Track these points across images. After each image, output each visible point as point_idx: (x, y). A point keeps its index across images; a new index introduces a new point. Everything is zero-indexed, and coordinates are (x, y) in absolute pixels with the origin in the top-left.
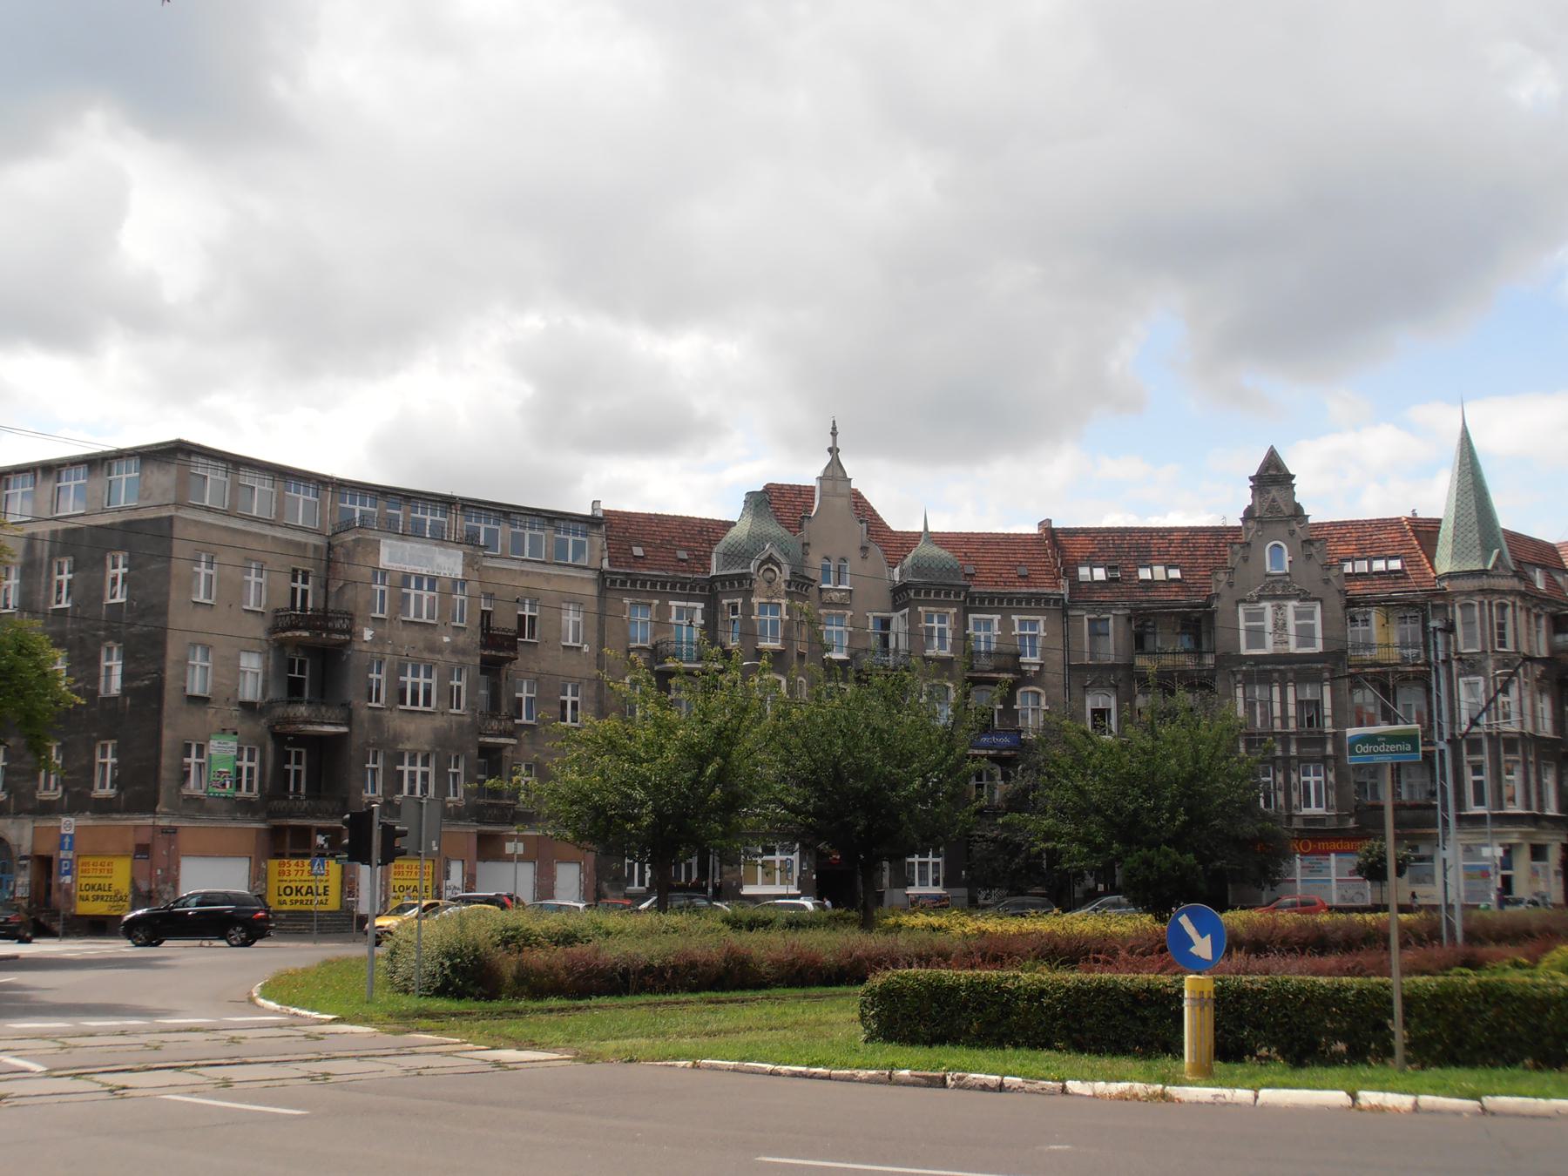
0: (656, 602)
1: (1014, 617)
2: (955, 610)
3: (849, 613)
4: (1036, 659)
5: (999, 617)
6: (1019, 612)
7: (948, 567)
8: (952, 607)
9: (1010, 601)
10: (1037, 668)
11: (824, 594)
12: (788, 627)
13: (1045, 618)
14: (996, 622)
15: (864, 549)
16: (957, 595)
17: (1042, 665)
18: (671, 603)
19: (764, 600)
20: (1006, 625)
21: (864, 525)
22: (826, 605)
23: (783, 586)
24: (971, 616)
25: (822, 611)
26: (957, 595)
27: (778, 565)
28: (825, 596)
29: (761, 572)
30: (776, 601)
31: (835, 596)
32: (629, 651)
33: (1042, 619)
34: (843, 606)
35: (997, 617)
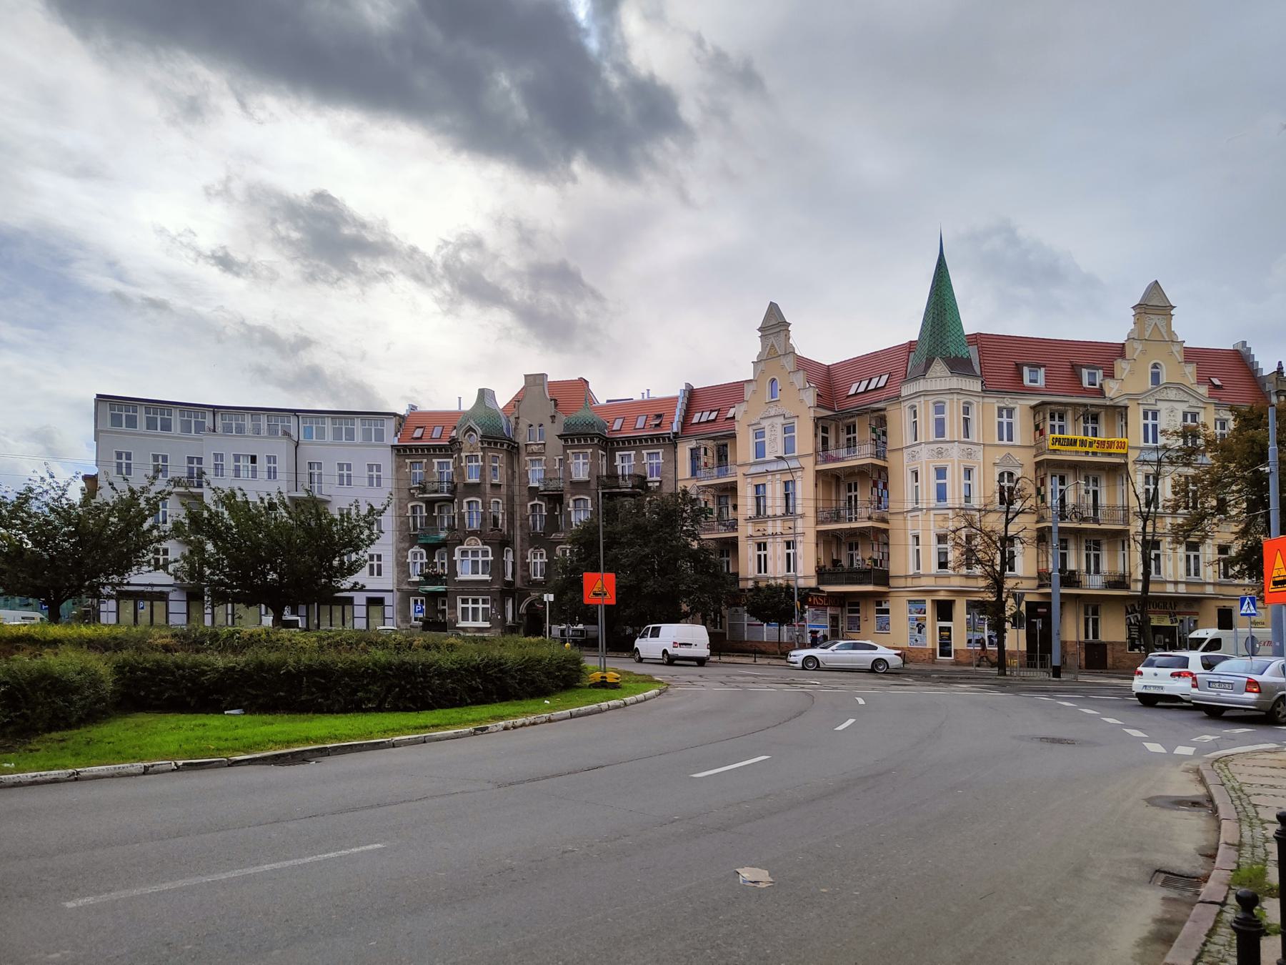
0: (425, 460)
1: (643, 452)
2: (591, 450)
3: (544, 458)
4: (659, 479)
5: (634, 452)
6: (647, 447)
7: (587, 422)
8: (589, 448)
9: (640, 441)
10: (658, 484)
11: (528, 448)
12: (483, 469)
13: (663, 450)
14: (632, 456)
15: (553, 417)
16: (592, 440)
17: (660, 482)
18: (434, 460)
19: (469, 454)
20: (639, 457)
21: (553, 402)
22: (529, 454)
23: (480, 445)
24: (617, 454)
25: (527, 458)
26: (592, 440)
27: (476, 434)
28: (529, 449)
29: (466, 436)
30: (474, 454)
31: (535, 448)
32: (410, 489)
33: (661, 451)
34: (541, 454)
35: (633, 453)
